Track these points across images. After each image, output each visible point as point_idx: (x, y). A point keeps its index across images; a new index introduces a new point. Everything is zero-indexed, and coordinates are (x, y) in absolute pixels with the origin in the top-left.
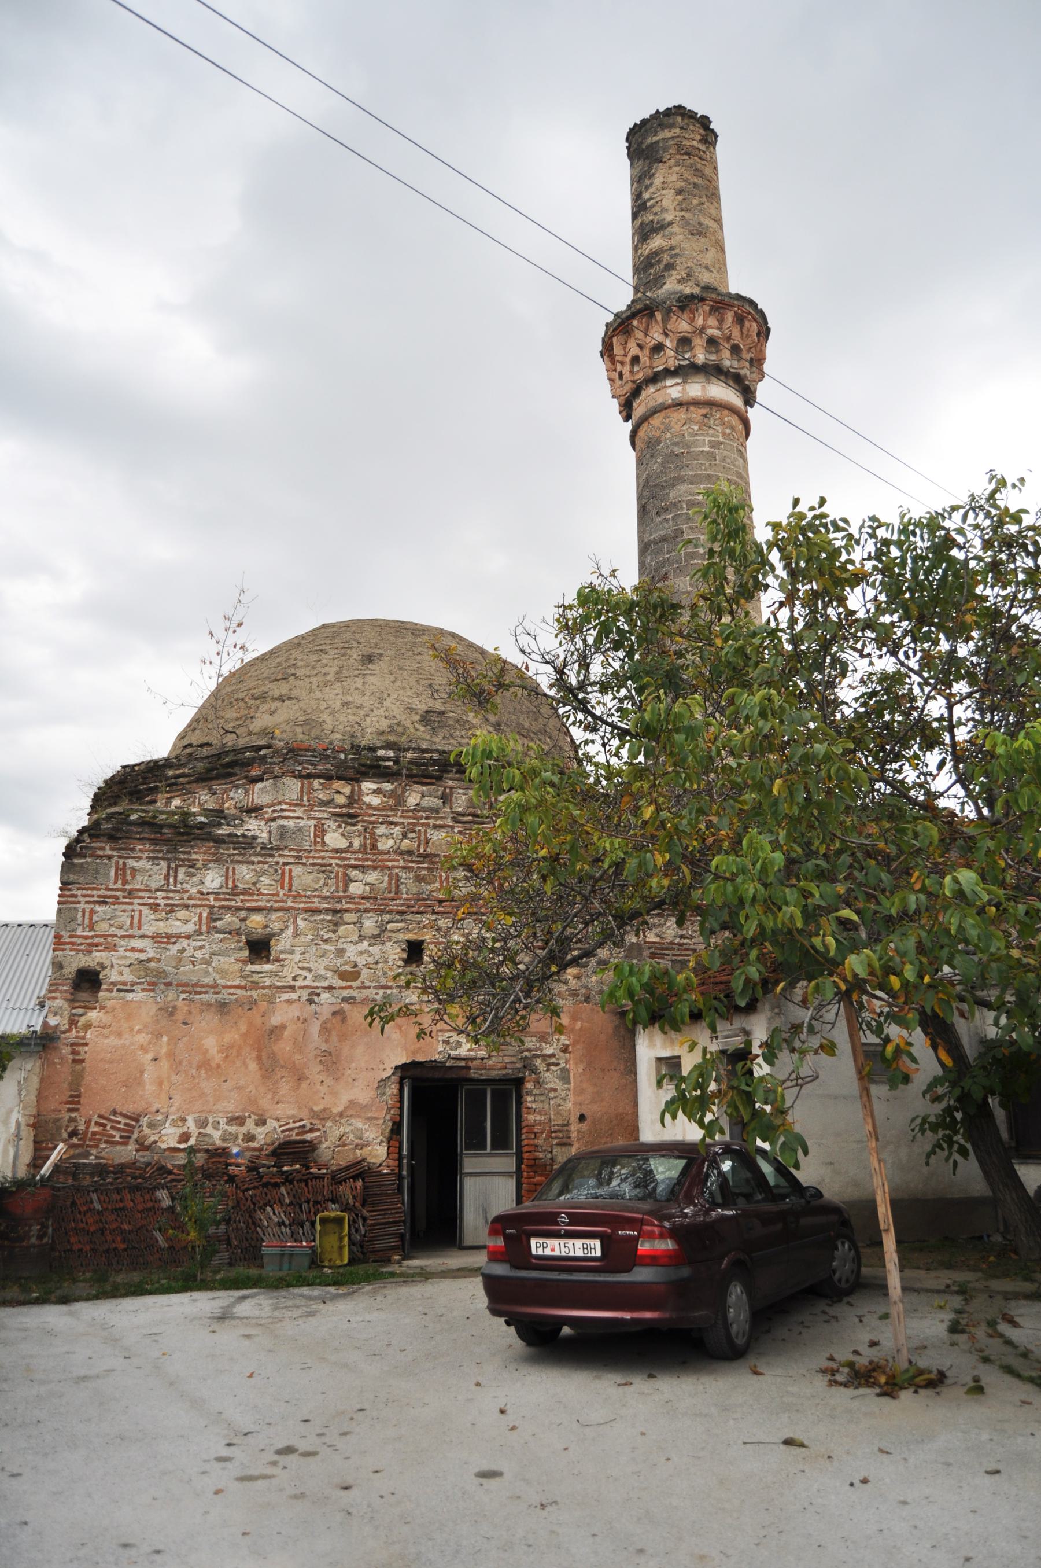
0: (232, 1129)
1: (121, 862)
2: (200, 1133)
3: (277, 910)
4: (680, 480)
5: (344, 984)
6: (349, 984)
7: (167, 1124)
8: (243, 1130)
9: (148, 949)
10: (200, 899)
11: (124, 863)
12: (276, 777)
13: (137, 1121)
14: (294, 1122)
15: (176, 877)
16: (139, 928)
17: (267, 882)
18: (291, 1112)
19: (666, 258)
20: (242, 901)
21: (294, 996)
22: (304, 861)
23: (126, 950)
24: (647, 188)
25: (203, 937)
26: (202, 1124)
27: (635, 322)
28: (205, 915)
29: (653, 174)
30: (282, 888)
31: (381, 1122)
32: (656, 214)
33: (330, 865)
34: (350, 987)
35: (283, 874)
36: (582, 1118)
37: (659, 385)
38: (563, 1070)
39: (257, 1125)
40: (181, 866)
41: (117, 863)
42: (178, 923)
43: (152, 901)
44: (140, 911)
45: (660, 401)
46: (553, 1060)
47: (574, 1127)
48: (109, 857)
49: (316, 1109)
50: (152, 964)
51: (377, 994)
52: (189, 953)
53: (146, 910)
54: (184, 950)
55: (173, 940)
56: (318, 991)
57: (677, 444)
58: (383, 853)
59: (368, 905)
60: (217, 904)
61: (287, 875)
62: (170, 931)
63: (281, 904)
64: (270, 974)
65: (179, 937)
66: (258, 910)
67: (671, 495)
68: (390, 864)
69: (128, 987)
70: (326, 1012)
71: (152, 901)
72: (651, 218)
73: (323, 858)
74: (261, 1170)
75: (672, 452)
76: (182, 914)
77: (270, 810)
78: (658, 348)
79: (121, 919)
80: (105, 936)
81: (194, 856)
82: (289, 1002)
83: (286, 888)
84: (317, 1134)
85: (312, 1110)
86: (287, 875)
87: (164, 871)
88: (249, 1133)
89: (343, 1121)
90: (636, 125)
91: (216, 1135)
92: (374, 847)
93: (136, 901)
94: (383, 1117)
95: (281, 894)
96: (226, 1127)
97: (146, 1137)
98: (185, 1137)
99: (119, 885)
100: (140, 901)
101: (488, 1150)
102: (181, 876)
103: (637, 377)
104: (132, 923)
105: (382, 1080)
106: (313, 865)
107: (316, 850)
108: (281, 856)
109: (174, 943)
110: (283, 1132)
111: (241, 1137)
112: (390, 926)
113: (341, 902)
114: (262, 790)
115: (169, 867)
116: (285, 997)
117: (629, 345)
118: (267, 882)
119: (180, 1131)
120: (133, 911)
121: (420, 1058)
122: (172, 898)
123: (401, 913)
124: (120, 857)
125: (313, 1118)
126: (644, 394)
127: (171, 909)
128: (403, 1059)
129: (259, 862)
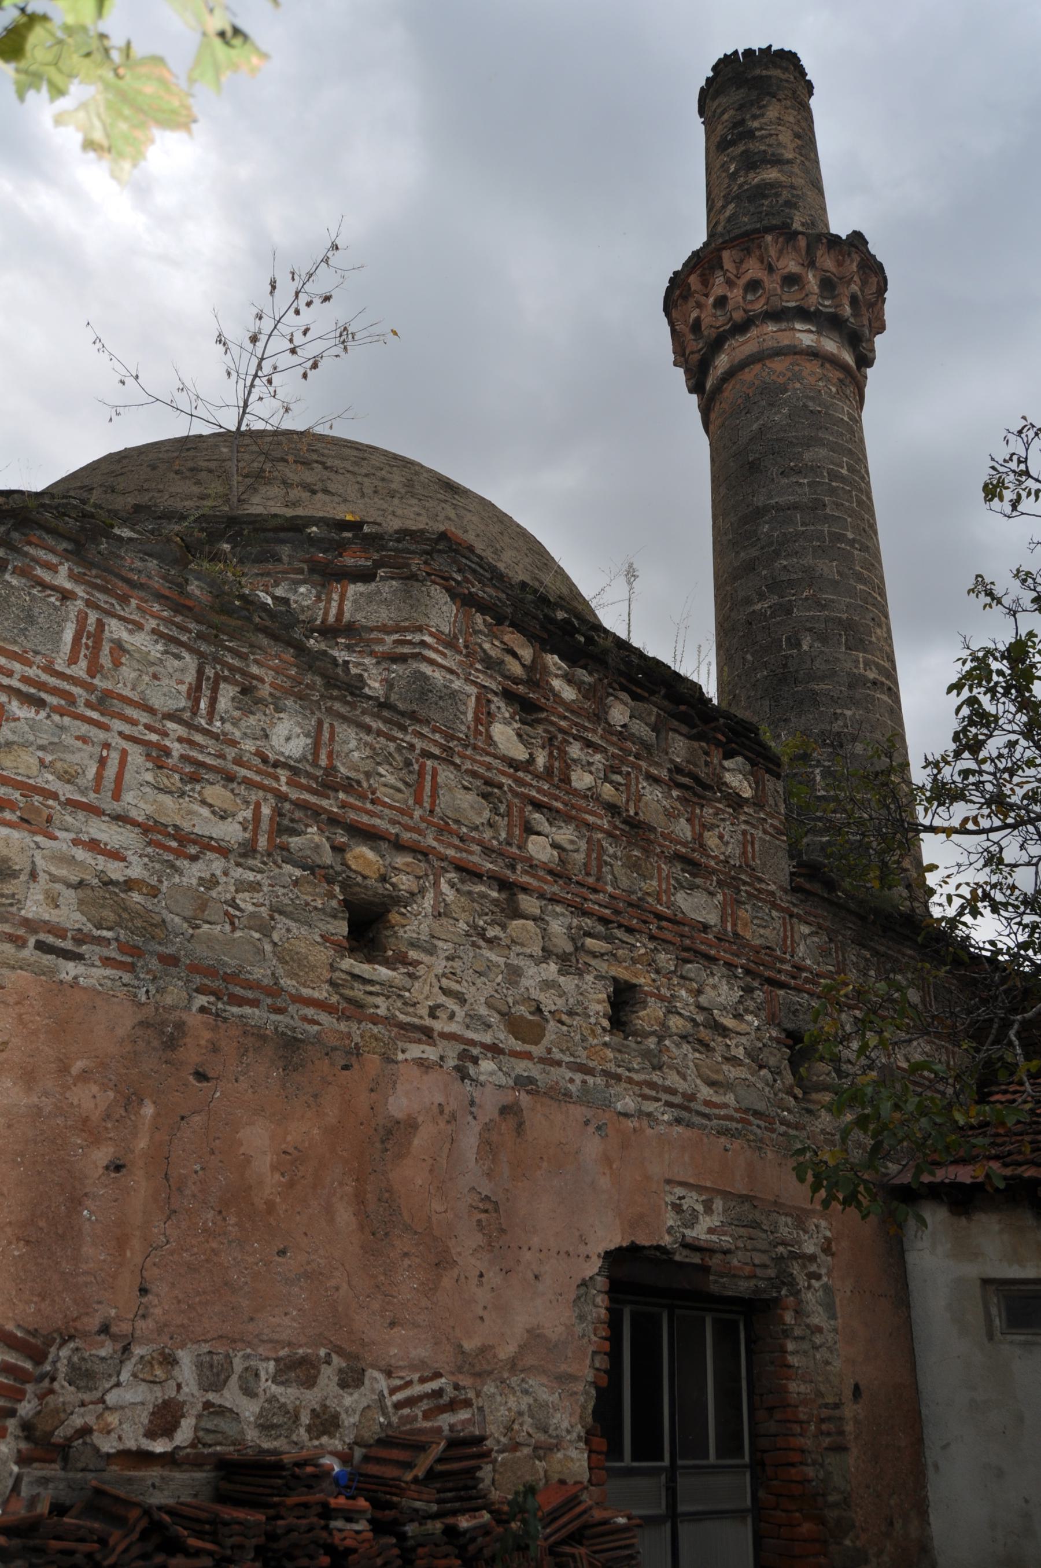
0: (288, 1394)
1: (93, 617)
2: (207, 1405)
3: (399, 846)
4: (821, 443)
5: (519, 1046)
6: (528, 1047)
7: (125, 1376)
8: (312, 1398)
9: (133, 859)
10: (259, 772)
11: (100, 625)
12: (413, 577)
13: (38, 1356)
14: (423, 1380)
15: (213, 701)
16: (117, 796)
17: (391, 779)
18: (421, 1352)
19: (785, 194)
20: (344, 805)
21: (431, 1053)
22: (458, 761)
23: (76, 842)
24: (755, 117)
25: (256, 863)
26: (214, 1376)
27: (769, 238)
28: (266, 811)
29: (764, 106)
30: (418, 801)
31: (579, 1387)
32: (770, 145)
33: (500, 786)
34: (528, 1056)
35: (421, 774)
36: (857, 1391)
37: (784, 325)
38: (826, 1288)
39: (343, 1385)
40: (226, 679)
41: (82, 620)
42: (205, 812)
43: (154, 737)
44: (124, 753)
45: (786, 342)
46: (813, 1268)
47: (849, 1411)
48: (66, 596)
49: (468, 1346)
50: (136, 897)
51: (572, 1081)
52: (225, 891)
53: (136, 756)
54: (212, 882)
55: (193, 850)
56: (475, 1051)
57: (812, 399)
58: (575, 792)
59: (555, 889)
60: (294, 794)
61: (428, 778)
62: (186, 826)
63: (415, 836)
64: (389, 990)
65: (207, 845)
66: (370, 836)
67: (807, 456)
68: (591, 819)
69: (68, 945)
70: (490, 1102)
71: (154, 737)
72: (763, 148)
73: (489, 767)
74: (410, 1529)
75: (805, 406)
76: (216, 793)
77: (390, 639)
78: (791, 280)
79: (75, 758)
80: (28, 789)
81: (255, 670)
82: (421, 1063)
83: (427, 805)
84: (464, 1415)
85: (460, 1349)
86: (428, 778)
87: (190, 677)
88: (325, 1407)
89: (514, 1381)
90: (736, 52)
91: (249, 1409)
92: (567, 780)
93: (117, 725)
94: (585, 1369)
95: (417, 814)
96: (275, 1389)
97: (62, 1413)
98: (165, 1418)
99: (80, 670)
100: (127, 729)
101: (712, 1459)
102: (223, 703)
103: (749, 307)
104: (99, 777)
105: (584, 1284)
106: (474, 774)
107: (475, 748)
108: (421, 735)
109: (194, 858)
110: (398, 1406)
111: (305, 1419)
112: (589, 941)
113: (513, 868)
114: (370, 598)
115: (200, 672)
116: (415, 1051)
117: (745, 266)
118: (391, 779)
119: (155, 1395)
120: (107, 746)
121: (643, 1241)
122: (201, 748)
123: (604, 921)
124: (90, 604)
125: (460, 1370)
126: (753, 332)
127: (195, 774)
128: (616, 1240)
129: (379, 733)
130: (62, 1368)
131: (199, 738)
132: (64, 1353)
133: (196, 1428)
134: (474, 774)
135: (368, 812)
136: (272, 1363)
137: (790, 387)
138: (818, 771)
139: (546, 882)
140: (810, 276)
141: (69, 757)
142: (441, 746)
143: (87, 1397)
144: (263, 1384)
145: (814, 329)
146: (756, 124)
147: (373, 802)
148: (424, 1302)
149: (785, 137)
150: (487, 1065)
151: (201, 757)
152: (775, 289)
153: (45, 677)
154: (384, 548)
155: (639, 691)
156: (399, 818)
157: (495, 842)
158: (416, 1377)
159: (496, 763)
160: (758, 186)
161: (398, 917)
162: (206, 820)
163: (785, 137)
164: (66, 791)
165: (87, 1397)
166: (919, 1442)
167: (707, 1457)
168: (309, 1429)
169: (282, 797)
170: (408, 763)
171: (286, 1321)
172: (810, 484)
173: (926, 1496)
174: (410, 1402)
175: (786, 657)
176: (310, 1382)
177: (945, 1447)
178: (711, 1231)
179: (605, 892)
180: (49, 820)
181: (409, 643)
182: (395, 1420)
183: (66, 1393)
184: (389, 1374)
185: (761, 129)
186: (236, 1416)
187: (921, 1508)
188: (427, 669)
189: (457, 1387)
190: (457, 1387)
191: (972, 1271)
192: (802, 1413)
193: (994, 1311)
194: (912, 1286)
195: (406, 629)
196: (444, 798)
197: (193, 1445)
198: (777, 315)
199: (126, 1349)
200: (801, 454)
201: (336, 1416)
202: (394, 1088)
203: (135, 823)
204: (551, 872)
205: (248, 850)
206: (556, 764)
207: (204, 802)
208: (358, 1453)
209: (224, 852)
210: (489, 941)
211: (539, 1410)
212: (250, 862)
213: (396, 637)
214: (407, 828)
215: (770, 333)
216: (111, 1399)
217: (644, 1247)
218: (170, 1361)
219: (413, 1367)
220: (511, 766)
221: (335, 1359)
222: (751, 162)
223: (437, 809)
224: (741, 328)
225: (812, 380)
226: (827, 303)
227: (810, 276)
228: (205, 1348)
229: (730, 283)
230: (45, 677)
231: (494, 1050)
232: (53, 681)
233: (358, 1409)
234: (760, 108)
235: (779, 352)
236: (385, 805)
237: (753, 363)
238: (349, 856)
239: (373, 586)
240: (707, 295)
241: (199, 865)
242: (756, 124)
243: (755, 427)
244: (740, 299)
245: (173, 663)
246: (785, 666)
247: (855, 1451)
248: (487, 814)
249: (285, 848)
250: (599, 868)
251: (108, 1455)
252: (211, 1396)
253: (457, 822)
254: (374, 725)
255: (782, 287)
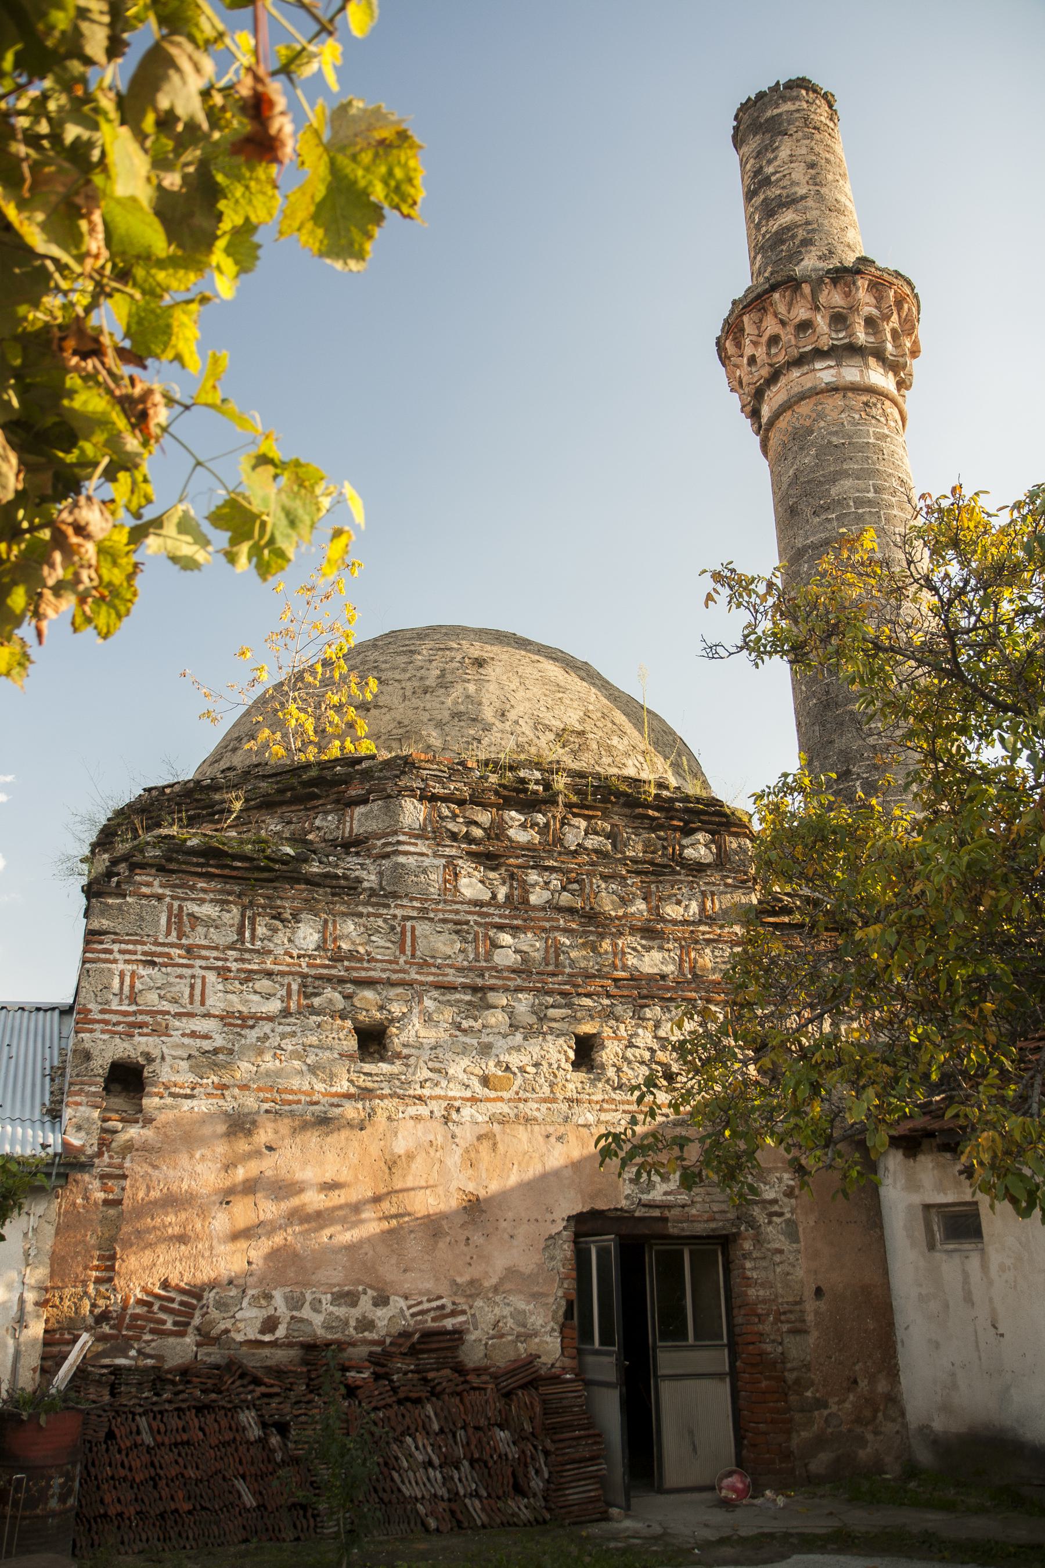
0: (341, 1311)
1: (176, 904)
2: (292, 1318)
3: (393, 984)
4: (845, 474)
5: (493, 1094)
6: (500, 1094)
7: (245, 1304)
8: (355, 1313)
9: (215, 1036)
10: (288, 965)
11: (180, 907)
12: (390, 796)
13: (199, 1298)
14: (429, 1301)
15: (253, 930)
16: (203, 1003)
17: (382, 943)
18: (429, 1285)
19: (801, 233)
20: (347, 969)
21: (423, 1110)
22: (432, 915)
23: (183, 1035)
24: (769, 162)
25: (293, 1020)
26: (295, 1303)
27: (776, 296)
28: (295, 987)
29: (777, 148)
30: (403, 951)
31: (551, 1300)
32: (784, 188)
33: (467, 923)
34: (501, 1099)
35: (403, 932)
36: (819, 1292)
37: (805, 369)
38: (788, 1222)
39: (376, 1305)
40: (259, 915)
41: (170, 907)
42: (256, 998)
43: (220, 963)
44: (204, 978)
45: (809, 385)
46: (776, 1208)
47: (810, 1306)
48: (160, 898)
49: (459, 1280)
50: (221, 1056)
51: (538, 1109)
52: (275, 1041)
53: (211, 977)
54: (266, 1037)
55: (251, 1023)
56: (457, 1104)
57: (836, 433)
58: (535, 908)
59: (519, 982)
60: (313, 972)
61: (409, 934)
62: (244, 1010)
63: (401, 975)
64: (391, 1078)
65: (258, 1018)
66: (369, 983)
67: (833, 492)
68: (547, 925)
69: (188, 1091)
70: (466, 1135)
71: (220, 963)
72: (778, 192)
73: (457, 912)
75: (830, 442)
76: (264, 984)
77: (379, 843)
78: (805, 326)
79: (177, 989)
80: (153, 1013)
81: (279, 902)
82: (417, 1118)
83: (409, 953)
84: (461, 1318)
85: (454, 1283)
86: (409, 934)
87: (236, 921)
88: (364, 1317)
89: (498, 1298)
90: (749, 99)
91: (318, 1319)
92: (525, 901)
93: (199, 963)
95: (401, 961)
96: (331, 1308)
97: (212, 1323)
98: (270, 1324)
99: (173, 938)
100: (203, 963)
101: (691, 1340)
102: (261, 931)
103: (775, 360)
104: (192, 996)
105: (551, 1237)
106: (444, 921)
107: (445, 902)
109: (252, 1027)
110: (413, 1315)
111: (353, 1323)
112: (551, 1012)
113: (482, 976)
114: (366, 815)
115: (243, 916)
116: (412, 1111)
117: (764, 325)
118: (382, 943)
119: (263, 1314)
120: (193, 977)
121: (601, 1205)
122: (249, 961)
123: (564, 994)
124: (173, 898)
125: (455, 1294)
126: (783, 381)
127: (248, 977)
128: (578, 1208)
129: (369, 915)
130: (211, 1302)
131: (247, 956)
132: (212, 1294)
133: (288, 1329)
134: (444, 921)
135: (364, 969)
136: (329, 1296)
137: (815, 428)
138: (858, 783)
139: (510, 979)
140: (819, 318)
141: (173, 989)
142: (418, 908)
143: (225, 1315)
144: (324, 1306)
145: (832, 363)
146: (770, 170)
147: (369, 961)
148: (426, 1257)
149: (799, 173)
150: (467, 1112)
151: (250, 967)
152: (789, 341)
153: (154, 948)
154: (372, 778)
155: (591, 813)
156: (389, 966)
157: (465, 963)
158: (425, 1299)
159: (466, 907)
160: (776, 233)
161: (394, 1030)
162: (258, 1003)
163: (799, 173)
164: (173, 1009)
165: (225, 1315)
166: (891, 1324)
167: (686, 1339)
168: (355, 1328)
169: (304, 976)
170: (393, 928)
171: (336, 1273)
172: (838, 518)
173: (897, 1364)
174: (422, 1313)
175: (827, 685)
176: (354, 1304)
177: (907, 1328)
178: (666, 1193)
179: (563, 973)
180: (167, 1027)
181: (390, 843)
182: (412, 1323)
183: (214, 1314)
184: (406, 1298)
185: (776, 172)
186: (310, 1323)
187: (893, 1373)
188: (402, 859)
189: (454, 1303)
190: (454, 1303)
191: (917, 1199)
192: (761, 1309)
193: (936, 1228)
194: (884, 1212)
195: (388, 835)
196: (421, 943)
197: (286, 1337)
198: (799, 361)
199: (244, 1291)
200: (828, 490)
201: (373, 1321)
202: (396, 1135)
203: (215, 1016)
204: (514, 971)
205: (286, 1013)
206: (516, 893)
207: (255, 992)
208: (388, 1340)
209: (270, 1019)
210: (464, 1031)
211: (520, 1316)
212: (288, 1021)
213: (383, 841)
214: (395, 971)
215: (795, 379)
216: (238, 1316)
217: (603, 1211)
218: (268, 1297)
219: (421, 1294)
220: (476, 905)
221: (369, 1292)
222: (770, 210)
223: (418, 953)
224: (773, 378)
225: (834, 415)
226: (841, 335)
227: (819, 318)
228: (288, 1289)
229: (755, 344)
230: (154, 948)
231: (474, 1100)
232: (159, 949)
233: (386, 1319)
234: (773, 151)
235: (802, 397)
236: (377, 961)
237: (781, 414)
238: (355, 1000)
239: (368, 807)
240: (742, 356)
241: (257, 1029)
242: (770, 170)
243: (791, 472)
244: (764, 356)
245: (226, 916)
246: (828, 693)
247: (815, 1334)
248: (458, 945)
249: (310, 1006)
250: (557, 956)
251: (241, 1343)
252: (295, 1313)
253: (433, 957)
254: (365, 911)
255: (796, 336)
